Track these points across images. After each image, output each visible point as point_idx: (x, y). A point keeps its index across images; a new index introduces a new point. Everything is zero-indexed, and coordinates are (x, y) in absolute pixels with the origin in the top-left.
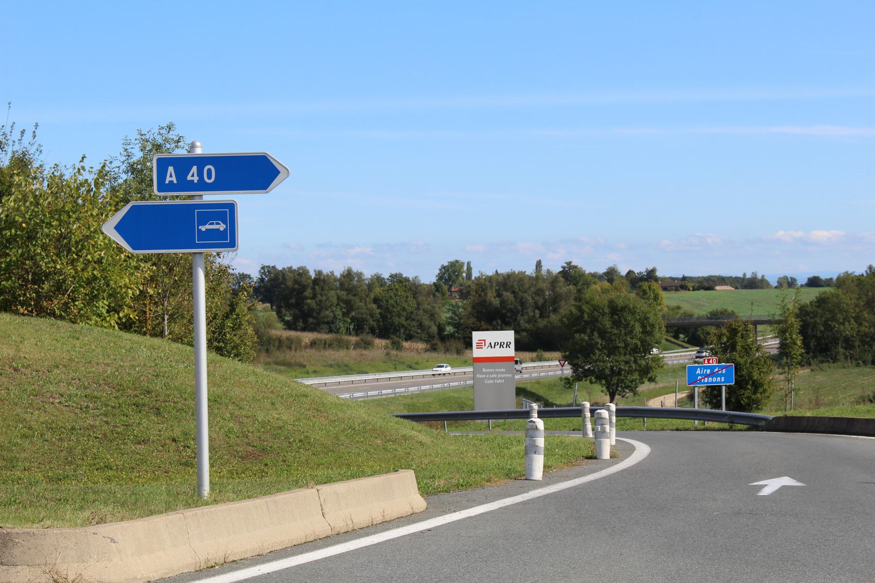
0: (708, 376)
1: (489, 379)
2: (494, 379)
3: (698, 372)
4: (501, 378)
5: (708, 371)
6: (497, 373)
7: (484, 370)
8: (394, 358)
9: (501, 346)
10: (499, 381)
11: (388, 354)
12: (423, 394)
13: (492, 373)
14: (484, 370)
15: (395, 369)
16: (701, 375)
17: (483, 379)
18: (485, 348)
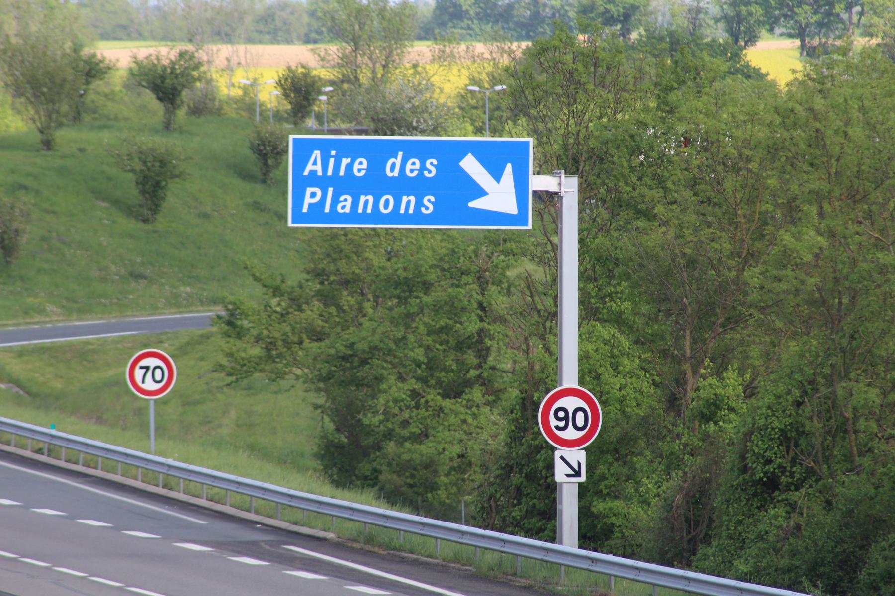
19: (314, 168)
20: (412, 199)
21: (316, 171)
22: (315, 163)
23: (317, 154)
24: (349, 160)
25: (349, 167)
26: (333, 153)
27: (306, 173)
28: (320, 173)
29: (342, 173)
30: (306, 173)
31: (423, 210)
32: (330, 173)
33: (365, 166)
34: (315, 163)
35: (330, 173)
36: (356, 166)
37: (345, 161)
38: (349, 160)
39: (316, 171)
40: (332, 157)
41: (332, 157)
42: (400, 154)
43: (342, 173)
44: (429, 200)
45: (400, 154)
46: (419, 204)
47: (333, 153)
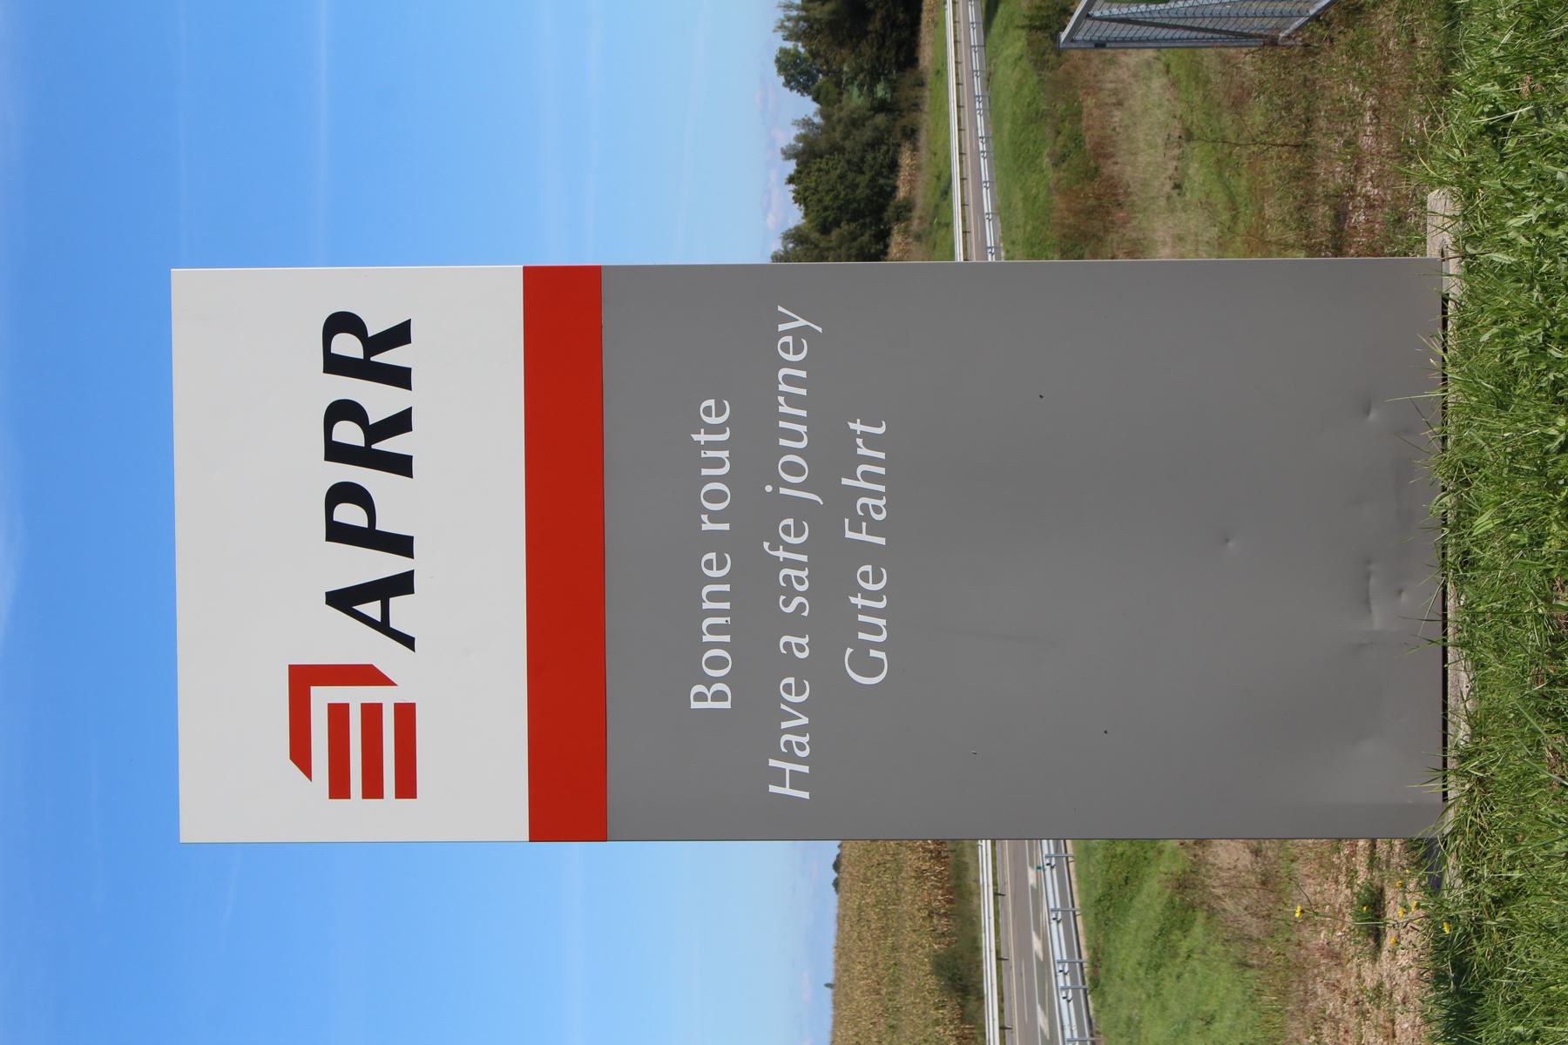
1: (832, 620)
2: (833, 565)
4: (832, 455)
6: (756, 512)
7: (710, 697)
8: (926, 225)
9: (374, 446)
10: (867, 483)
11: (918, 238)
12: (1003, 211)
13: (755, 585)
14: (710, 697)
15: (949, 225)
17: (832, 706)
18: (408, 679)
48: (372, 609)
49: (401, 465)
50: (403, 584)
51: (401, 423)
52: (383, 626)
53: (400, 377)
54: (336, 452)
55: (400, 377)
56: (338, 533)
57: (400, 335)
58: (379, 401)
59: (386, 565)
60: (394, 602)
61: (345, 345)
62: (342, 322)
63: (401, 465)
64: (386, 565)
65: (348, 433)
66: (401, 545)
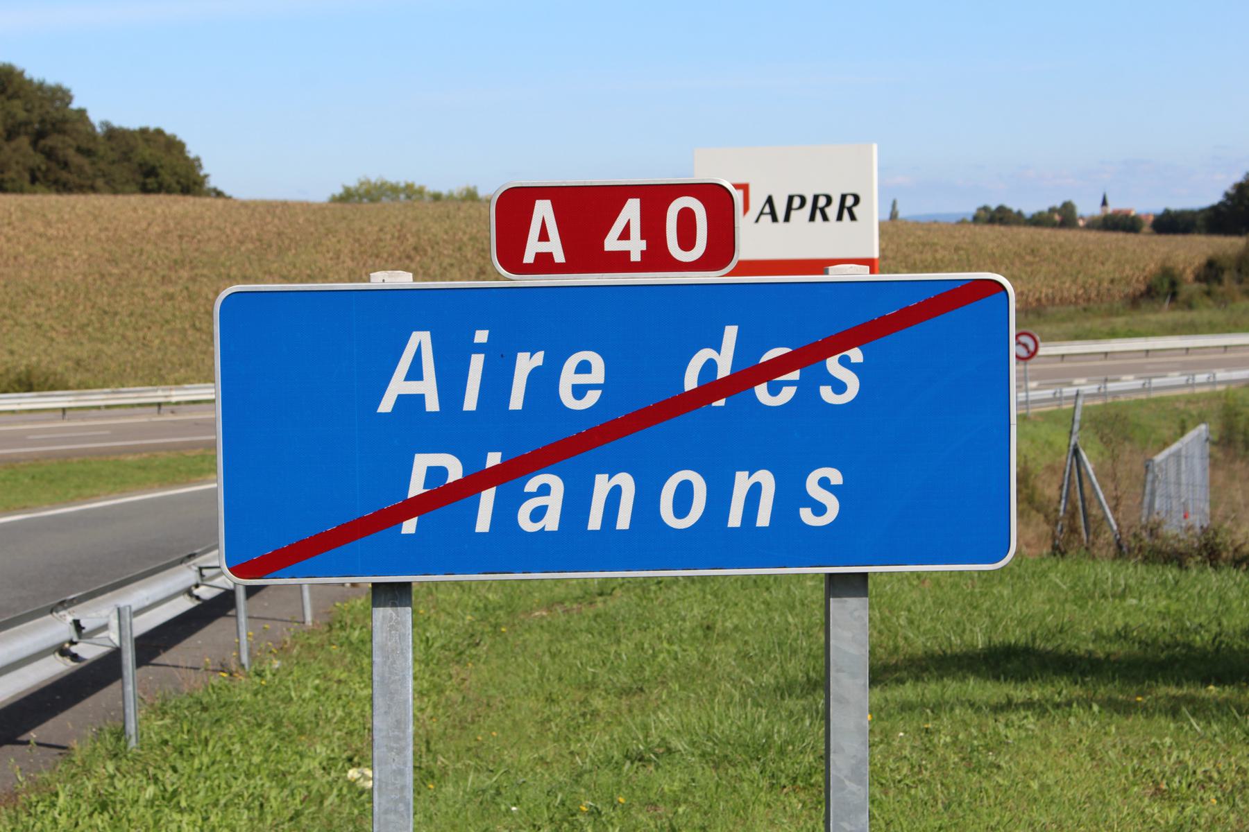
0: (573, 447)
3: (413, 380)
5: (583, 382)
9: (818, 210)
16: (446, 429)
19: (413, 388)
20: (766, 478)
21: (420, 398)
22: (415, 373)
23: (421, 340)
24: (539, 359)
25: (543, 381)
26: (481, 336)
27: (386, 405)
28: (432, 405)
29: (516, 402)
30: (386, 405)
31: (806, 515)
32: (470, 402)
33: (598, 374)
34: (415, 373)
35: (470, 402)
36: (568, 377)
37: (526, 363)
38: (539, 359)
39: (420, 398)
40: (479, 348)
41: (479, 348)
42: (731, 334)
43: (516, 402)
44: (824, 483)
45: (731, 334)
46: (791, 495)
47: (481, 336)
48: (767, 210)
49: (812, 218)
50: (775, 219)
51: (825, 218)
52: (762, 213)
53: (840, 218)
54: (816, 198)
55: (840, 218)
56: (791, 199)
57: (853, 218)
58: (832, 211)
59: (781, 213)
60: (769, 218)
61: (849, 201)
62: (857, 199)
63: (812, 218)
64: (781, 213)
65: (822, 202)
66: (787, 219)
